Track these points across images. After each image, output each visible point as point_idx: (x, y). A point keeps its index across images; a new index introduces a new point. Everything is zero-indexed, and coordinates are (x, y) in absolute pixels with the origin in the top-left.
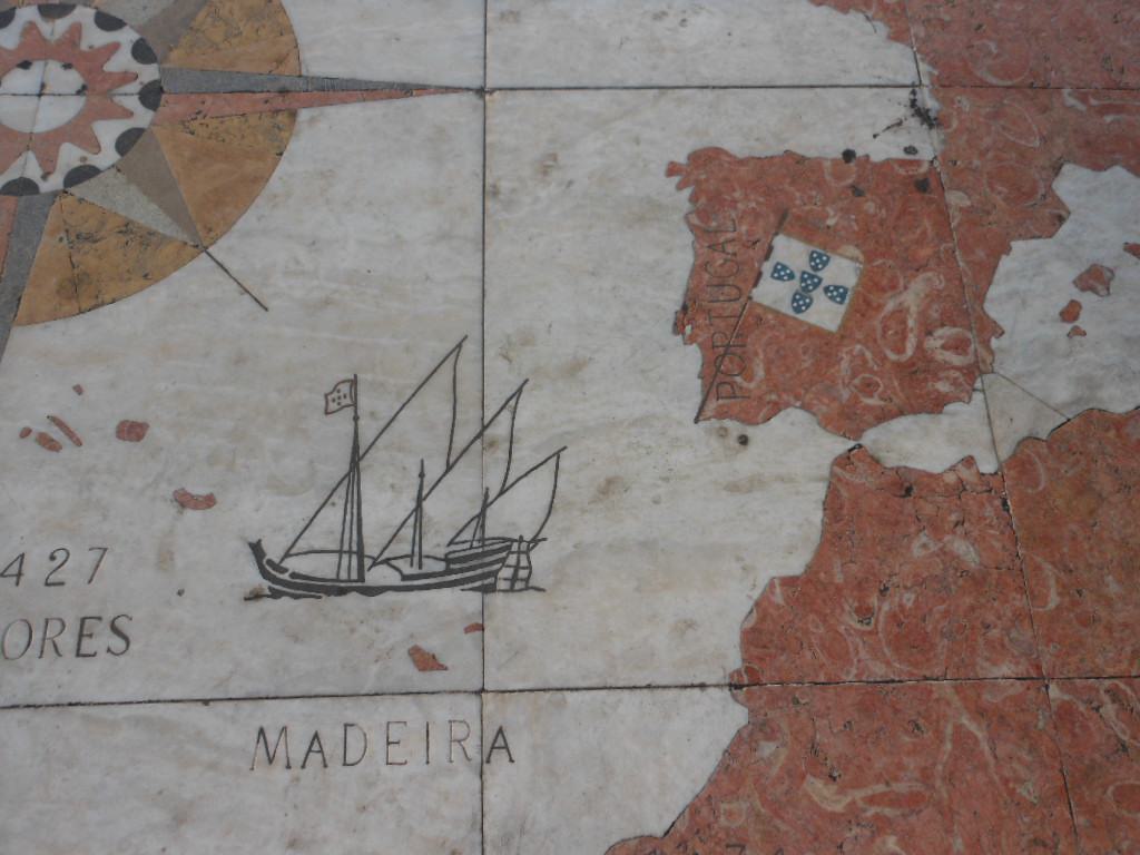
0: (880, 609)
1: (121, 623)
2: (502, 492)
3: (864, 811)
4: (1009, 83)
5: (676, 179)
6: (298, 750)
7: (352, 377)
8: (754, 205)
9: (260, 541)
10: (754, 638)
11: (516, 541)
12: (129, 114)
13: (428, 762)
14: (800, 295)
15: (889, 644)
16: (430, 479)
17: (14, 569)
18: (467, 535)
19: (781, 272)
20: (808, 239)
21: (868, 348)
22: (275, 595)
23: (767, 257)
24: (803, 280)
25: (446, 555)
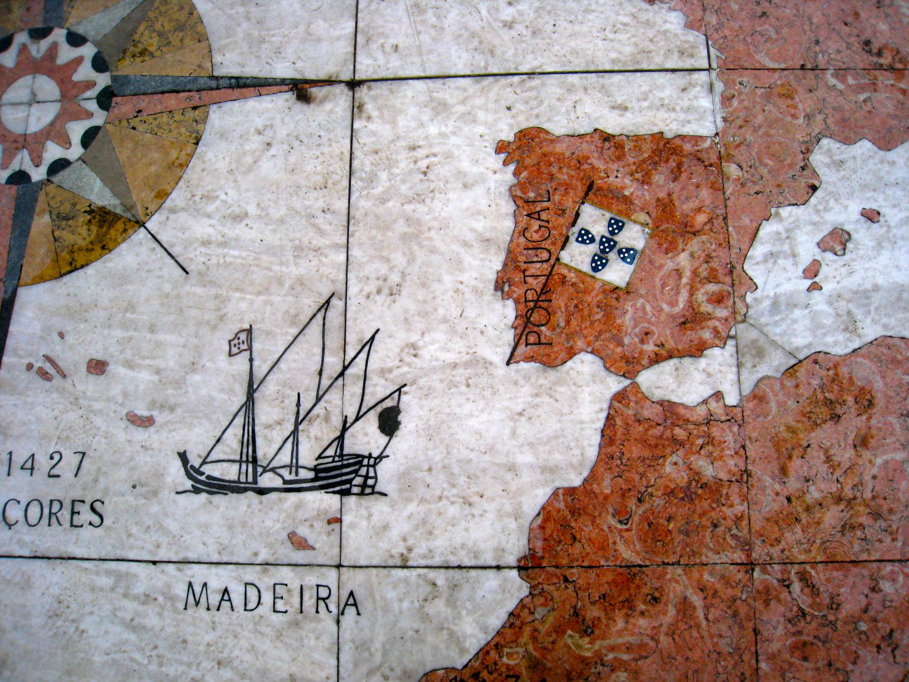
1: (98, 506)
2: (357, 418)
3: (606, 655)
4: (783, 66)
5: (503, 156)
6: (215, 599)
7: (248, 327)
8: (566, 177)
9: (185, 452)
11: (366, 457)
12: (90, 115)
13: (301, 612)
14: (598, 256)
16: (306, 405)
17: (29, 465)
18: (331, 452)
19: (585, 237)
20: (608, 208)
21: (649, 302)
22: (196, 491)
23: (574, 224)
24: (601, 243)
25: (315, 466)
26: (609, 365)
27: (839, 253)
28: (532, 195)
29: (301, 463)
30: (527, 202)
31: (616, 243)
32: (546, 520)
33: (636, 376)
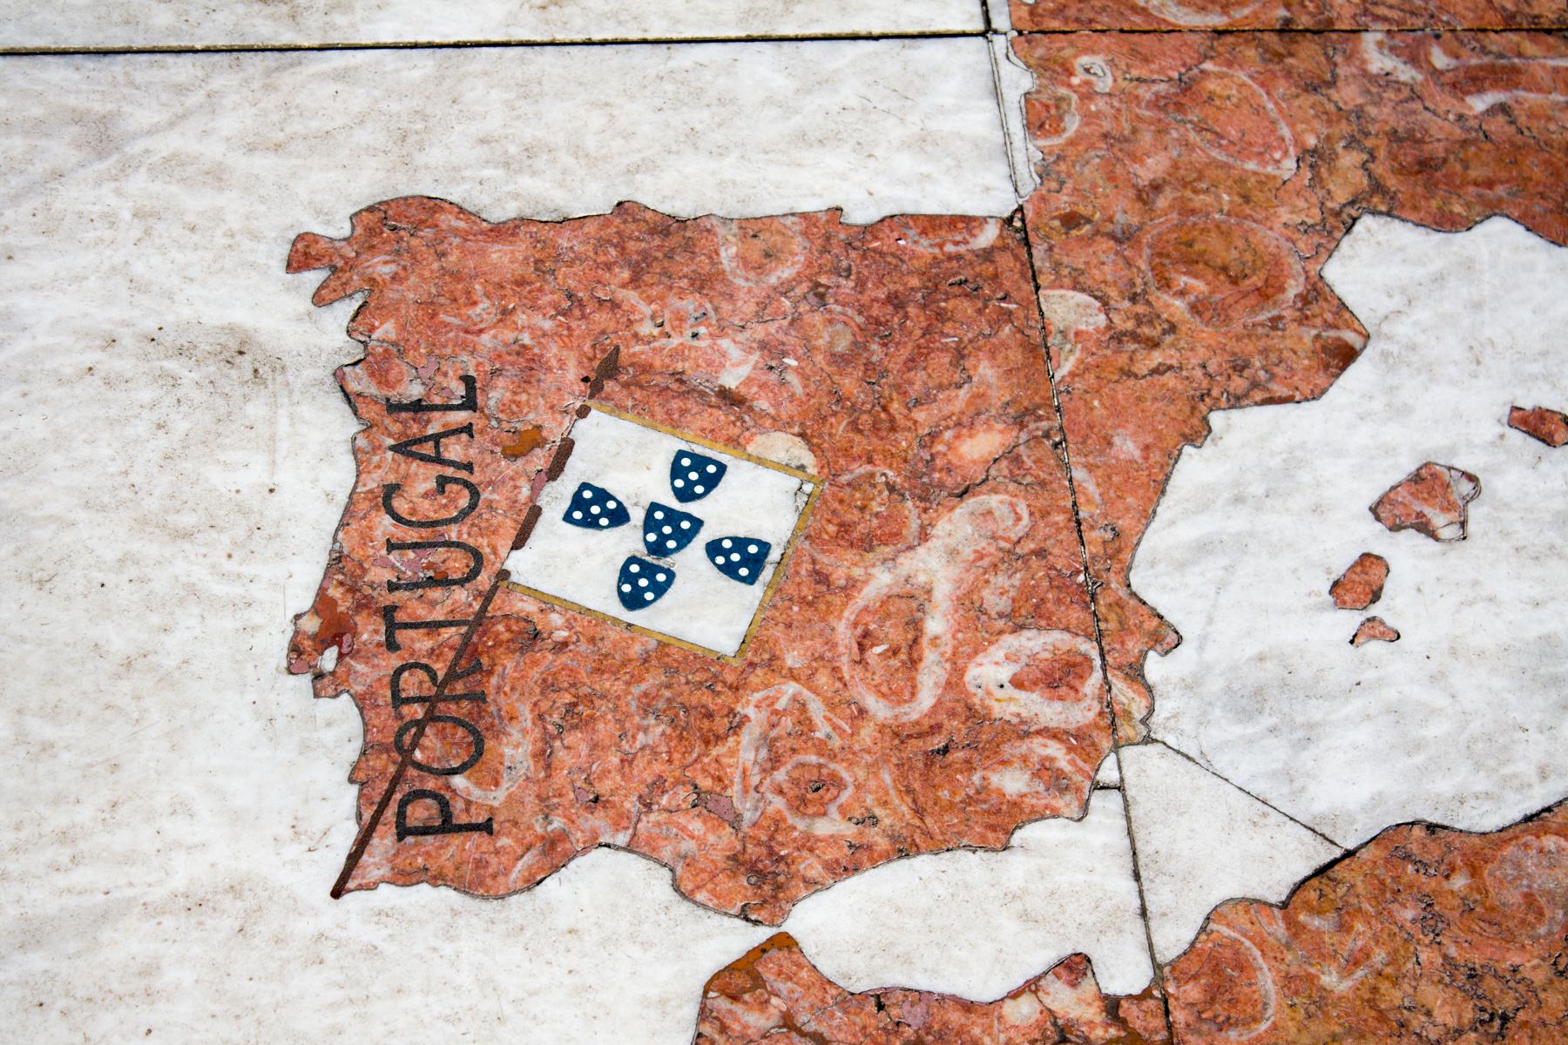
4: (1217, 20)
5: (313, 278)
20: (673, 424)
23: (555, 470)
24: (650, 524)
27: (1445, 533)
28: (415, 391)
30: (394, 408)
31: (697, 524)
33: (785, 914)
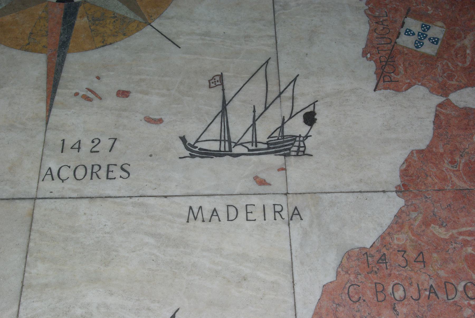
0: (460, 162)
1: (125, 167)
2: (291, 118)
6: (207, 216)
7: (220, 74)
8: (395, 6)
9: (184, 136)
10: (404, 173)
11: (298, 137)
15: (465, 175)
16: (259, 112)
17: (77, 146)
18: (276, 134)
19: (409, 33)
20: (421, 19)
21: (449, 62)
22: (192, 156)
23: (402, 26)
24: (419, 35)
26: (433, 91)
29: (258, 140)
31: (427, 35)
32: (408, 166)
33: (448, 96)
